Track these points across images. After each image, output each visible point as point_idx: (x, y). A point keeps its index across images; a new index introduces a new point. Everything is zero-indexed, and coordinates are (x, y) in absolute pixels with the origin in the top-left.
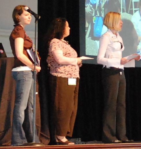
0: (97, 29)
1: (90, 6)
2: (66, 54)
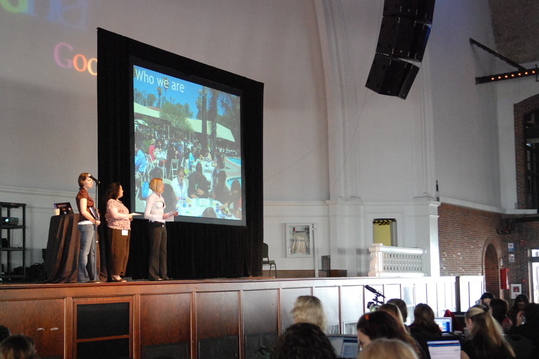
0: (144, 192)
1: (139, 173)
2: (120, 211)
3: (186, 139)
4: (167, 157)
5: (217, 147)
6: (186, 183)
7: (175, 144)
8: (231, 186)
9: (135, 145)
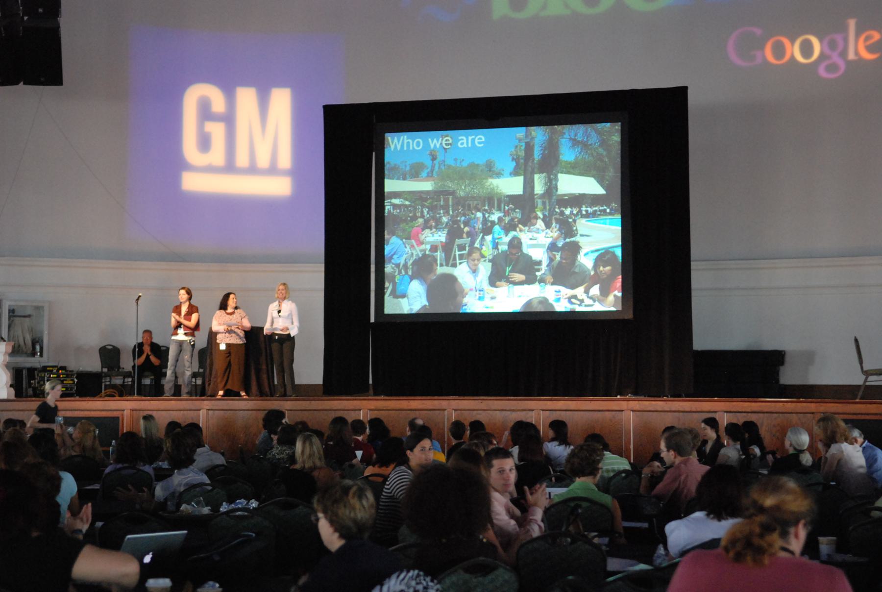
0: (400, 289)
3: (486, 208)
4: (446, 239)
5: (559, 208)
6: (485, 269)
7: (463, 218)
8: (594, 261)
9: (386, 231)
